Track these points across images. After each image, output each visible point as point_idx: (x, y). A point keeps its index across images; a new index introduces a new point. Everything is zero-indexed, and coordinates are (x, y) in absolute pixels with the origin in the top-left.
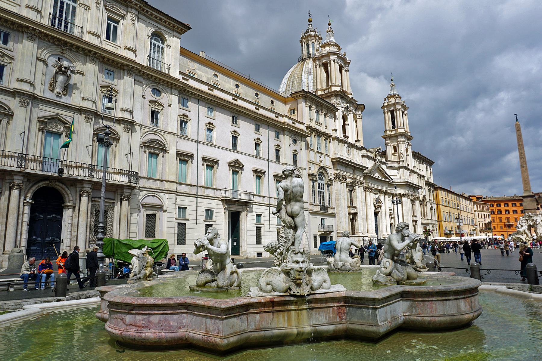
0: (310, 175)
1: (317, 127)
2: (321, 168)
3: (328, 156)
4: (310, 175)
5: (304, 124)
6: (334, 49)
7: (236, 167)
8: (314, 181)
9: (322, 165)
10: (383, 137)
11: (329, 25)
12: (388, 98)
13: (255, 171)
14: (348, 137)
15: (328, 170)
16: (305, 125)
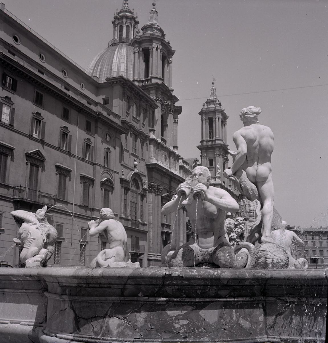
0: (122, 180)
1: (134, 124)
2: (136, 174)
3: (144, 160)
4: (122, 180)
5: (120, 117)
6: (157, 33)
7: (35, 160)
8: (127, 190)
9: (136, 170)
10: (198, 147)
11: (154, 5)
12: (207, 103)
13: (58, 167)
14: (165, 141)
15: (143, 178)
16: (121, 119)
